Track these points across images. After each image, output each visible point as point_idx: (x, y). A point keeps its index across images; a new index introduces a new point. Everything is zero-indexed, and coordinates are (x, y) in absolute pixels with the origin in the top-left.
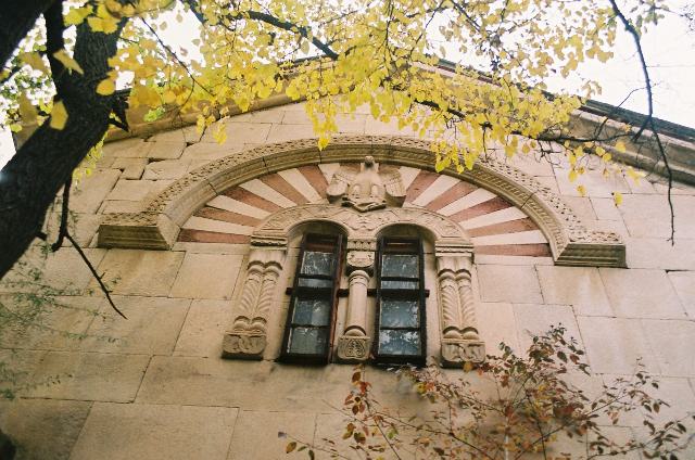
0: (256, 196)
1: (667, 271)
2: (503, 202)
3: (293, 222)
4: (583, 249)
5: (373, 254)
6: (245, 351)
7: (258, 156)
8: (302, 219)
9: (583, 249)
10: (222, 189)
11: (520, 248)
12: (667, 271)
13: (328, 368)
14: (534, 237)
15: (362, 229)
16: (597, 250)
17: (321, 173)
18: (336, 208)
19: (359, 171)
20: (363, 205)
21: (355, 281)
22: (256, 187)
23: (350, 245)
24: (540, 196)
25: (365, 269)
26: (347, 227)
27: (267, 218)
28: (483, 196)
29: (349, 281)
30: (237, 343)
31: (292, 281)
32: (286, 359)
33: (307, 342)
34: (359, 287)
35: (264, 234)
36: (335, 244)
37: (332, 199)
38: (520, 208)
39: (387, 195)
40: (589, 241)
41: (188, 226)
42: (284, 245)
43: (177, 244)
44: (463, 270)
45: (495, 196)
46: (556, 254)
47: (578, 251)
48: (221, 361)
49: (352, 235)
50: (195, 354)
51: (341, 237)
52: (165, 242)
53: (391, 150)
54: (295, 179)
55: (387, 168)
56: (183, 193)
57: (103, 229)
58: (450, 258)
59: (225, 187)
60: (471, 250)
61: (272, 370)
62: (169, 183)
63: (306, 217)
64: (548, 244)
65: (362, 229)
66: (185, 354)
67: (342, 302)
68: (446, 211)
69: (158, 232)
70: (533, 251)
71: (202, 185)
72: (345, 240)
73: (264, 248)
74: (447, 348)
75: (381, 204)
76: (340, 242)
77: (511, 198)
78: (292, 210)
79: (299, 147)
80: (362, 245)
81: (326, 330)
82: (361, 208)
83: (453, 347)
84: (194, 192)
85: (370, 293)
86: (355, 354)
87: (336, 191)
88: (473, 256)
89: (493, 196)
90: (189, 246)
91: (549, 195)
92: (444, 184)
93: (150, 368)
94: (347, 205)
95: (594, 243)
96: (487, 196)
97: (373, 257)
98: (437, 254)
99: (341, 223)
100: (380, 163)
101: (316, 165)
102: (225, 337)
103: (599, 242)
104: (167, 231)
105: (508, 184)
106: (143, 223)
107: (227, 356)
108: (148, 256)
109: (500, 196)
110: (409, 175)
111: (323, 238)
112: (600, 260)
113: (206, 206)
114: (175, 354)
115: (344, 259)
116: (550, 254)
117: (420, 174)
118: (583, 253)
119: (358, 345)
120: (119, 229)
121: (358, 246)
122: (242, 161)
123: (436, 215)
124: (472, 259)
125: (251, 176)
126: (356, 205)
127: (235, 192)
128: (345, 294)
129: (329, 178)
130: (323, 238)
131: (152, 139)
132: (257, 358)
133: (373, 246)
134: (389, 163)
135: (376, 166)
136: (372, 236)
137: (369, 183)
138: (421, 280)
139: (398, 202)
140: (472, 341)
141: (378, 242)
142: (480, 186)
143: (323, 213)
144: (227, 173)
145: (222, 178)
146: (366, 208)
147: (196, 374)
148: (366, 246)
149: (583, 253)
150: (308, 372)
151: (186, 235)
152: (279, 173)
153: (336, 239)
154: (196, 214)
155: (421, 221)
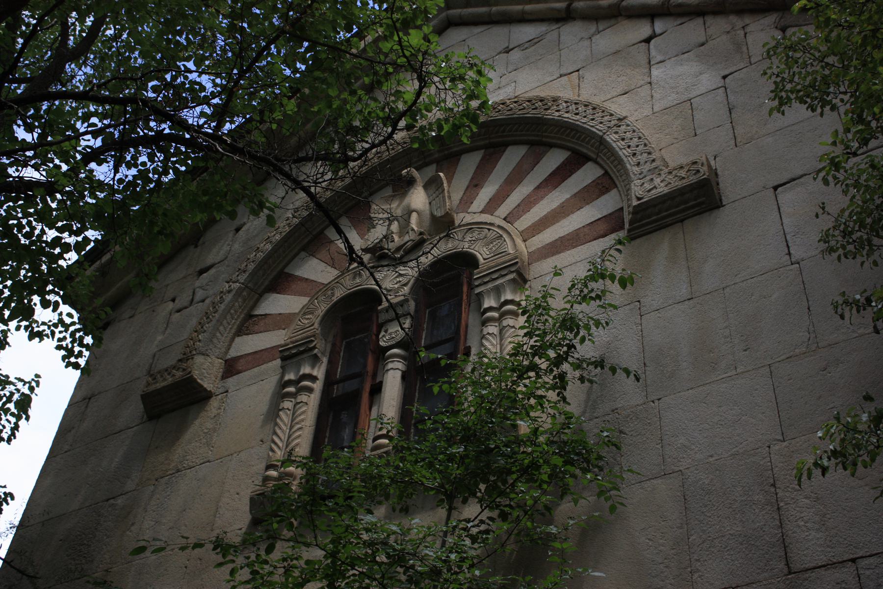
1: (775, 188)
2: (575, 162)
8: (335, 299)
11: (586, 230)
12: (775, 188)
21: (390, 366)
24: (611, 138)
28: (554, 160)
40: (662, 189)
41: (233, 353)
44: (507, 302)
57: (146, 398)
59: (266, 283)
60: (513, 269)
70: (602, 227)
73: (295, 360)
77: (585, 151)
80: (396, 313)
95: (666, 190)
96: (554, 160)
98: (477, 291)
103: (677, 184)
109: (574, 152)
112: (684, 210)
120: (158, 392)
131: (201, 242)
142: (551, 146)
154: (239, 332)
155: (465, 246)
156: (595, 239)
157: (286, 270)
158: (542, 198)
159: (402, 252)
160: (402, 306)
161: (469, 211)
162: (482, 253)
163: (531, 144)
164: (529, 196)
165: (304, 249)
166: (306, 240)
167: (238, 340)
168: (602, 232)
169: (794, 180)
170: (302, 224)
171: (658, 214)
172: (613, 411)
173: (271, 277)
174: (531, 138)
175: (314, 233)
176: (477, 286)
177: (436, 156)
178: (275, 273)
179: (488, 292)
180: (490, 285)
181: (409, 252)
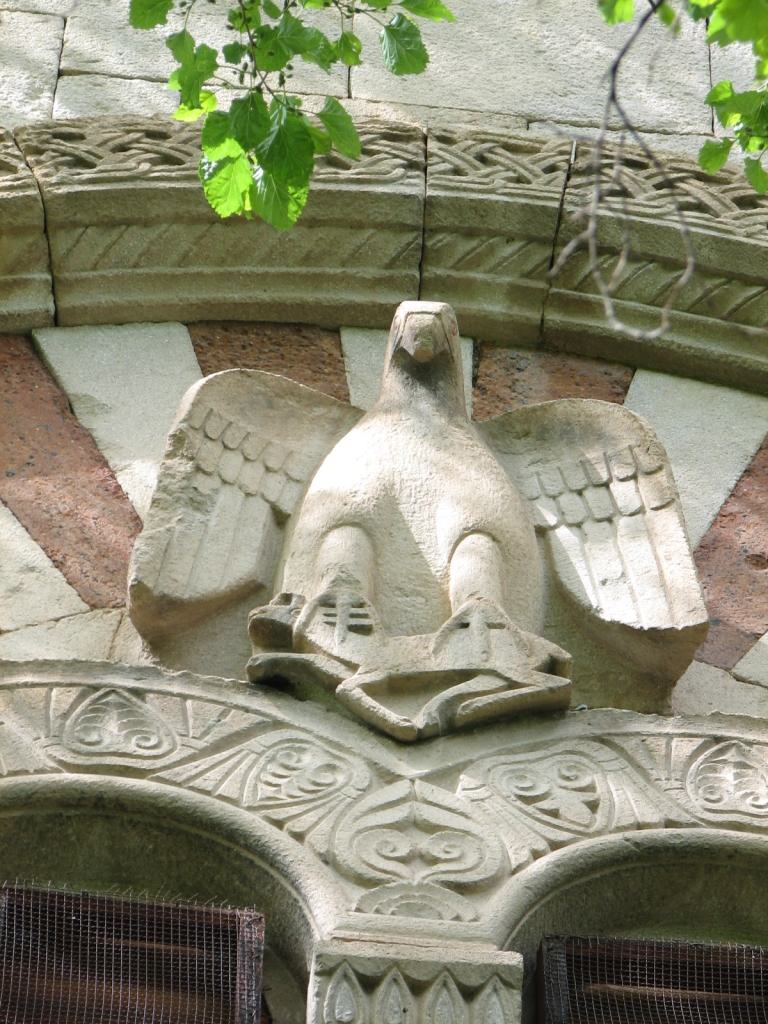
17: (66, 406)
19: (347, 413)
20: (402, 686)
26: (279, 841)
37: (170, 625)
39: (567, 613)
55: (531, 382)
75: (541, 683)
94: (288, 679)
99: (256, 824)
126: (351, 684)
134: (545, 342)
136: (479, 935)
146: (420, 715)
160: (469, 994)
161: (743, 668)
181: (457, 728)
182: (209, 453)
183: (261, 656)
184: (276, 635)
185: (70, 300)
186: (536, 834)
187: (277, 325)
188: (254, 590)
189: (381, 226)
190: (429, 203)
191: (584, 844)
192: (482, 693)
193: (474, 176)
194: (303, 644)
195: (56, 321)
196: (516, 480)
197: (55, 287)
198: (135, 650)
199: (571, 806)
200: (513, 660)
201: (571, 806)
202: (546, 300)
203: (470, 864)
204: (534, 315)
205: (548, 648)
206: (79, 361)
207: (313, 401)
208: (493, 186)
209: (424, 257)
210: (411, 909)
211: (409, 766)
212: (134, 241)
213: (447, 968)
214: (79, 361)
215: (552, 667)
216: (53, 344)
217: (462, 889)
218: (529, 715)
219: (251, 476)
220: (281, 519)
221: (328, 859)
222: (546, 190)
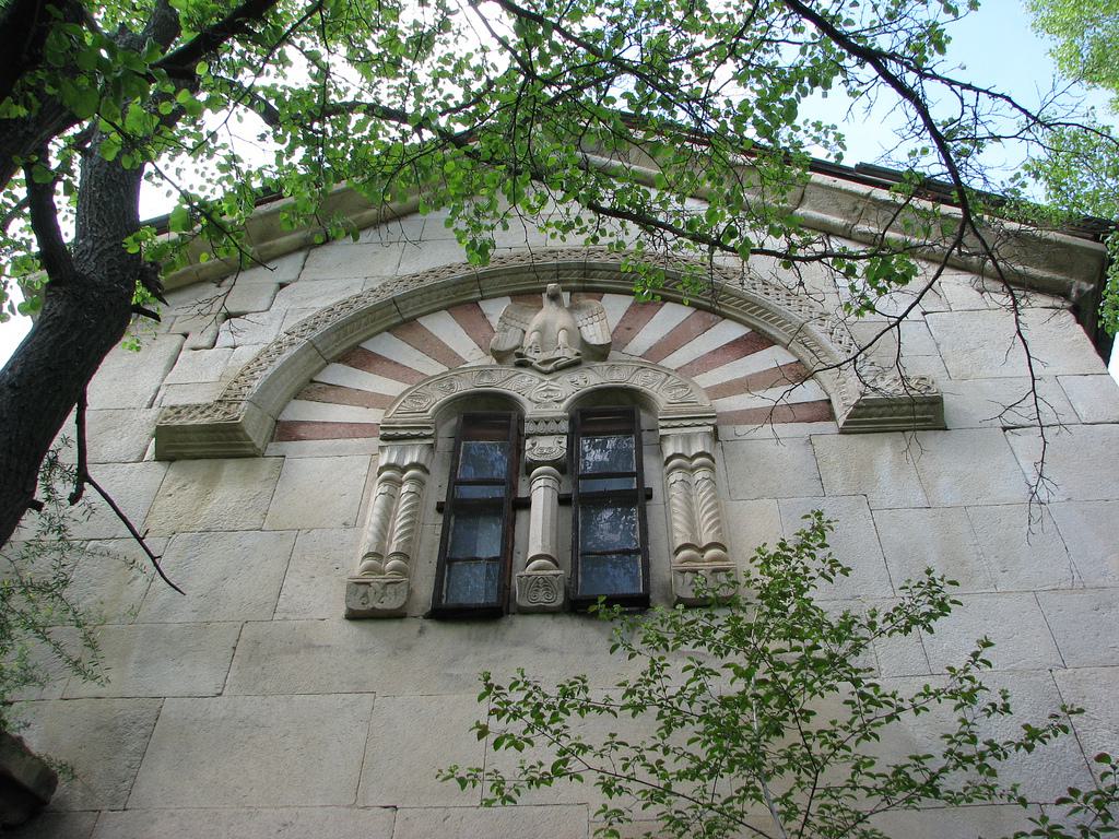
0: (389, 361)
2: (758, 340)
3: (440, 397)
4: (880, 407)
5: (564, 440)
6: (379, 606)
7: (385, 296)
9: (880, 407)
10: (333, 355)
12: (1005, 429)
13: (504, 622)
14: (808, 392)
15: (545, 398)
16: (900, 405)
17: (484, 316)
18: (508, 370)
20: (546, 362)
22: (389, 346)
23: (529, 428)
25: (553, 463)
26: (520, 397)
27: (403, 393)
28: (730, 331)
29: (531, 483)
30: (365, 595)
31: (444, 491)
32: (445, 613)
33: (474, 587)
34: (541, 495)
35: (400, 420)
36: (507, 427)
37: (500, 356)
38: (786, 347)
39: (584, 344)
41: (287, 416)
42: (429, 437)
43: (271, 445)
45: (747, 330)
46: (842, 415)
47: (873, 410)
48: (347, 622)
49: (530, 410)
50: (308, 616)
51: (514, 417)
52: (253, 445)
53: (586, 270)
54: (446, 329)
55: (584, 300)
56: (277, 364)
58: (677, 437)
61: (421, 632)
62: (257, 350)
63: (463, 387)
64: (829, 401)
65: (545, 398)
66: (289, 616)
67: (521, 515)
68: (675, 360)
69: (243, 431)
70: (806, 413)
71: (304, 350)
72: (521, 420)
74: (680, 580)
76: (514, 423)
77: (772, 332)
78: (441, 378)
79: (446, 276)
80: (546, 427)
81: (504, 562)
82: (544, 368)
83: (689, 576)
84: (292, 361)
85: (564, 501)
86: (542, 598)
87: (508, 341)
88: (716, 430)
89: (747, 330)
90: (290, 447)
91: (828, 324)
92: (670, 317)
93: (241, 641)
94: (523, 364)
96: (730, 331)
97: (564, 445)
98: (662, 432)
100: (572, 291)
101: (475, 303)
102: (349, 586)
104: (256, 433)
105: (767, 311)
106: (218, 417)
107: (353, 616)
108: (230, 467)
109: (755, 329)
110: (615, 307)
111: (486, 418)
113: (312, 381)
114: (277, 616)
115: (520, 450)
116: (831, 417)
117: (633, 305)
118: (880, 411)
119: (547, 584)
120: (183, 429)
121: (541, 428)
122: (361, 306)
123: (658, 370)
124: (715, 436)
125: (380, 328)
126: (535, 363)
127: (356, 356)
128: (526, 504)
129: (495, 321)
130: (486, 418)
132: (397, 615)
133: (564, 426)
134: (585, 290)
135: (566, 296)
136: (559, 410)
137: (551, 324)
138: (639, 474)
139: (600, 353)
140: (718, 565)
141: (572, 420)
142: (725, 317)
143: (485, 380)
144: (341, 329)
145: (334, 337)
146: (550, 367)
147: (310, 646)
148: (552, 427)
149: (880, 411)
150: (475, 630)
151: (286, 431)
152: (421, 321)
153: (509, 418)
154: (297, 396)
155: (638, 381)
156: (804, 421)
157: (363, 345)
158: (721, 364)
159: (550, 367)
160: (558, 423)
162: (664, 397)
163: (698, 307)
164: (703, 358)
165: (388, 330)
166: (394, 322)
167: (294, 402)
168: (806, 417)
169: (1023, 427)
170: (394, 301)
171: (881, 416)
172: (854, 597)
173: (345, 347)
174: (699, 301)
175: (405, 316)
176: (662, 428)
177: (574, 284)
178: (350, 343)
179: (677, 437)
180: (677, 431)
181: (558, 369)
182: (508, 320)
183: (517, 360)
184: (520, 355)
185: (485, 294)
186: (573, 388)
187: (523, 294)
188: (517, 347)
189: (549, 271)
190: (558, 265)
191: (583, 390)
192: (563, 361)
193: (568, 258)
194: (526, 356)
195: (482, 299)
196: (574, 318)
197: (481, 292)
198: (494, 362)
199: (581, 382)
200: (569, 354)
201: (581, 382)
202: (584, 282)
203: (560, 396)
204: (581, 285)
205: (576, 351)
206: (486, 306)
207: (531, 307)
208: (572, 259)
209: (558, 276)
210: (546, 407)
211: (547, 378)
212: (497, 280)
213: (552, 418)
214: (486, 306)
215: (578, 354)
216: (481, 303)
217: (557, 401)
218: (573, 365)
219: (517, 324)
220: (525, 332)
221: (530, 399)
222: (582, 259)
